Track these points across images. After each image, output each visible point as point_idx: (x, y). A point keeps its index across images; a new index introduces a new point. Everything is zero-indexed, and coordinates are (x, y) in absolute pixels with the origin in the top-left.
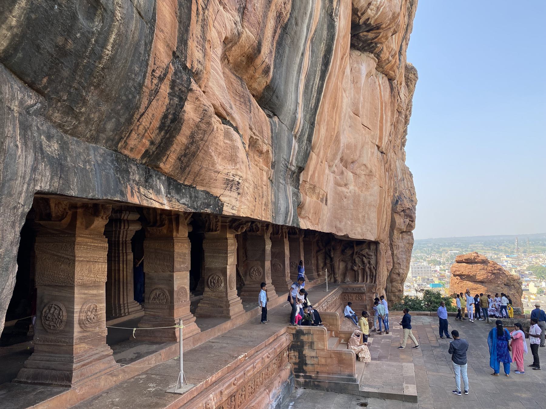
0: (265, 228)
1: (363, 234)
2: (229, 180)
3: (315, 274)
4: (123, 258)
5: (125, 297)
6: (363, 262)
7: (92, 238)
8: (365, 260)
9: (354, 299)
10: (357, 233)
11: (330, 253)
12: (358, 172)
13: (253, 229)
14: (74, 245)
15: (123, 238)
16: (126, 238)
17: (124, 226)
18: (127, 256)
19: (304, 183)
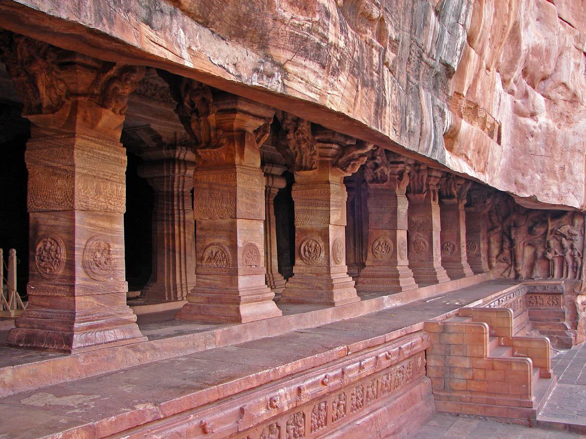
0: (397, 177)
1: (561, 197)
2: (302, 37)
3: (485, 265)
4: (180, 217)
5: (183, 274)
6: (562, 247)
7: (101, 144)
8: (566, 243)
9: (546, 302)
10: (550, 195)
11: (510, 232)
12: (553, 95)
13: (377, 178)
14: (73, 148)
15: (178, 187)
16: (183, 187)
17: (180, 169)
18: (184, 215)
19: (456, 98)
